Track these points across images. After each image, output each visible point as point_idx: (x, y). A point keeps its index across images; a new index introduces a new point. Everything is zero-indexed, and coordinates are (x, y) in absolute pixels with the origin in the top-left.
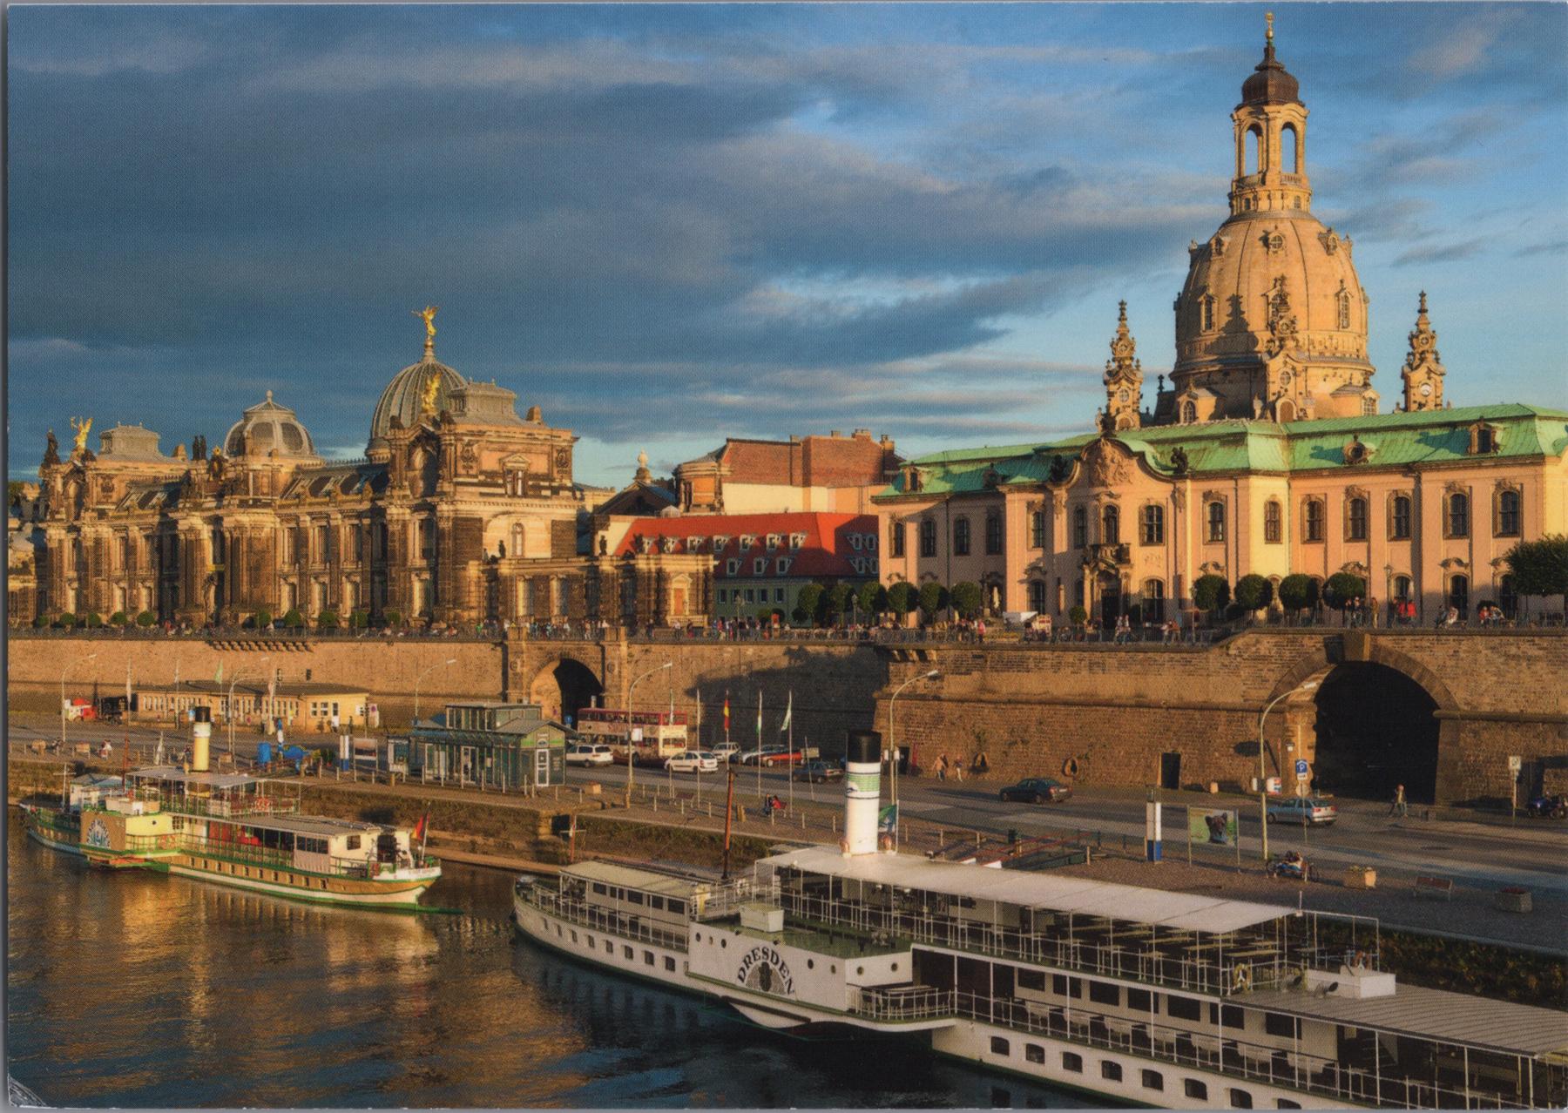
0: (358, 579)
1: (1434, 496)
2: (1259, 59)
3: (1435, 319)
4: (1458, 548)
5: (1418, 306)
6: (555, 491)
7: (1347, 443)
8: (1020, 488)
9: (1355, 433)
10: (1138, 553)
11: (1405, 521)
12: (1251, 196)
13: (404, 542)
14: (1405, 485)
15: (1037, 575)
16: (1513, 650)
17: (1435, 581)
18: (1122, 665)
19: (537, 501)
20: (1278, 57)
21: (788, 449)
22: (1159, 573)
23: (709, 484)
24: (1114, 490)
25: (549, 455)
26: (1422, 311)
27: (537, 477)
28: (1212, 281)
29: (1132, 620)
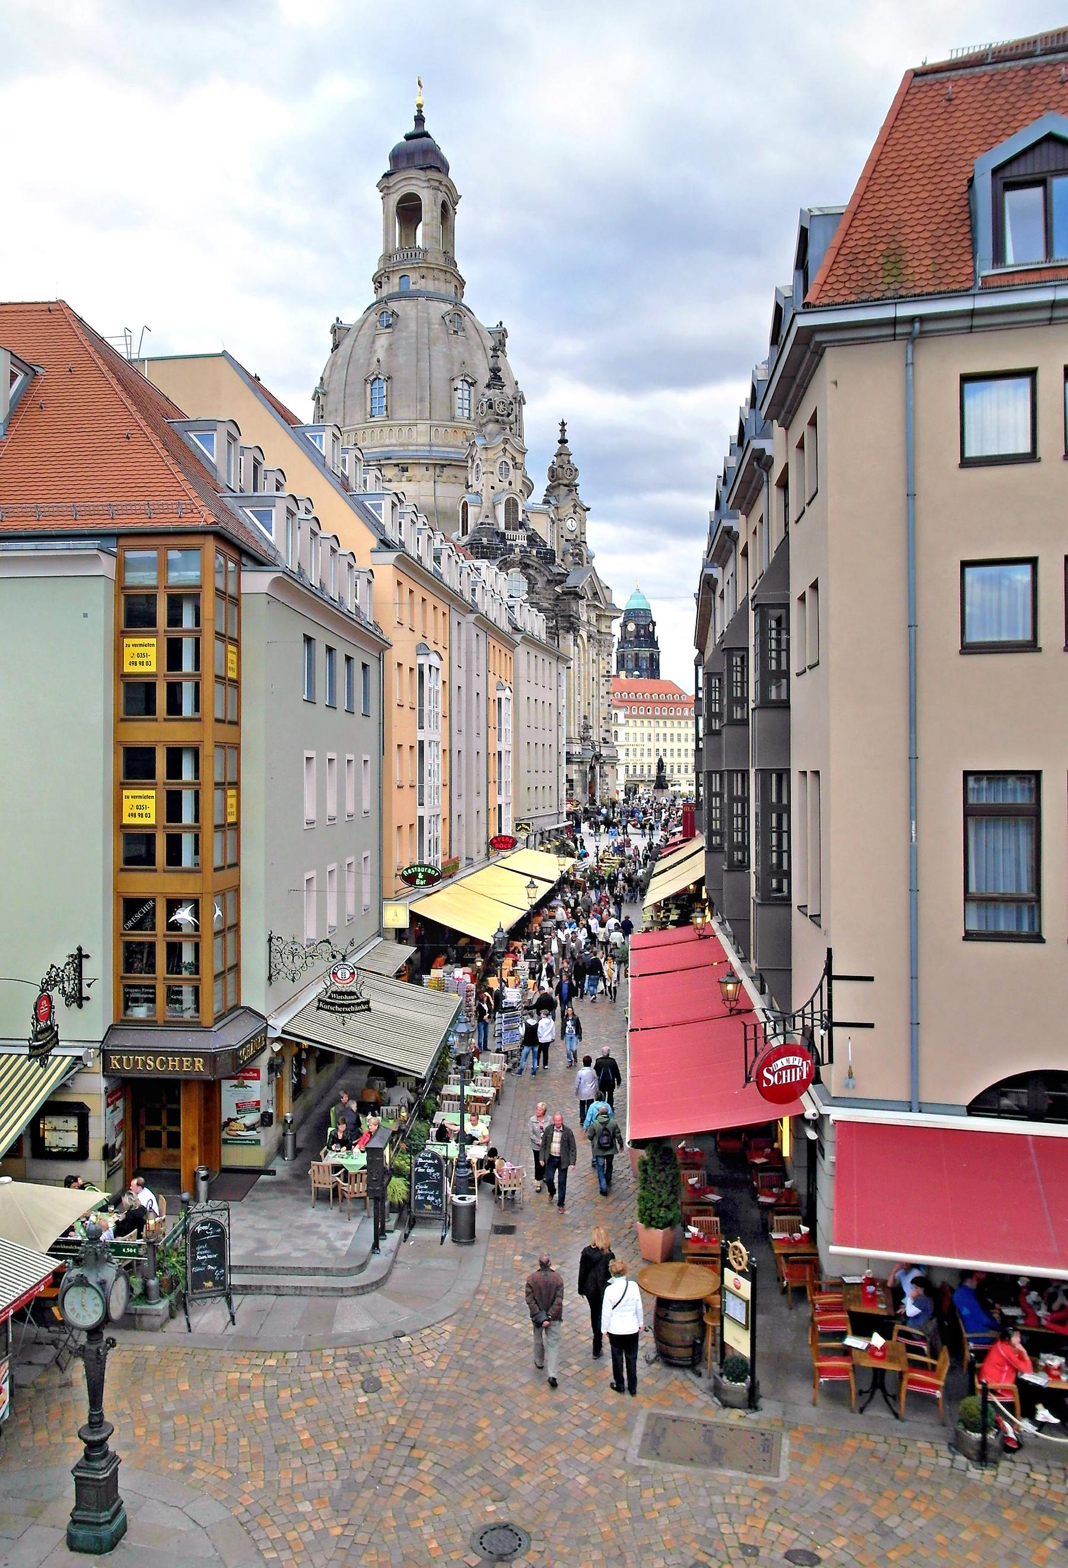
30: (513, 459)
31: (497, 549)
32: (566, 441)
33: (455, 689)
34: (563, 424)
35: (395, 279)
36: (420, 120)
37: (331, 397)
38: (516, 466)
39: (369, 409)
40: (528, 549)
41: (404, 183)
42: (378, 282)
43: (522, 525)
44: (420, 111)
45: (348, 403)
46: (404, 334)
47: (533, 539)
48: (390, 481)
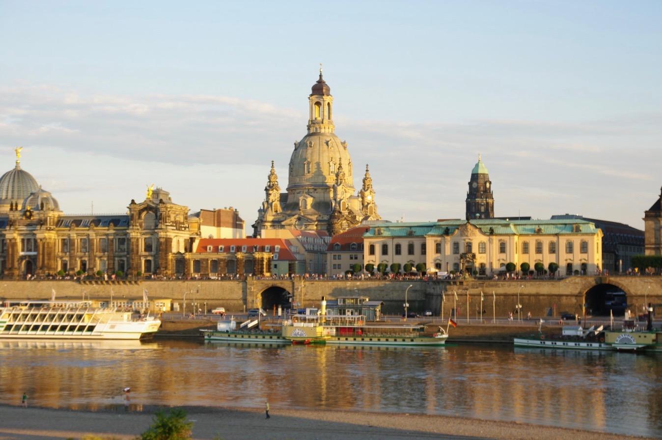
0: (106, 259)
1: (563, 242)
2: (318, 79)
3: (371, 174)
4: (570, 256)
5: (366, 169)
6: (185, 228)
7: (537, 228)
8: (433, 236)
9: (539, 225)
10: (478, 256)
11: (553, 249)
12: (318, 127)
13: (137, 246)
14: (554, 239)
15: (438, 262)
16: (646, 281)
17: (563, 264)
18: (531, 285)
19: (181, 232)
20: (324, 79)
21: (213, 213)
22: (484, 261)
23: (196, 225)
24: (471, 238)
25: (184, 215)
26: (367, 171)
27: (180, 223)
28: (309, 156)
29: (482, 274)
30: (345, 190)
36: (321, 76)
38: (346, 192)
42: (309, 128)
47: (350, 212)
48: (311, 193)
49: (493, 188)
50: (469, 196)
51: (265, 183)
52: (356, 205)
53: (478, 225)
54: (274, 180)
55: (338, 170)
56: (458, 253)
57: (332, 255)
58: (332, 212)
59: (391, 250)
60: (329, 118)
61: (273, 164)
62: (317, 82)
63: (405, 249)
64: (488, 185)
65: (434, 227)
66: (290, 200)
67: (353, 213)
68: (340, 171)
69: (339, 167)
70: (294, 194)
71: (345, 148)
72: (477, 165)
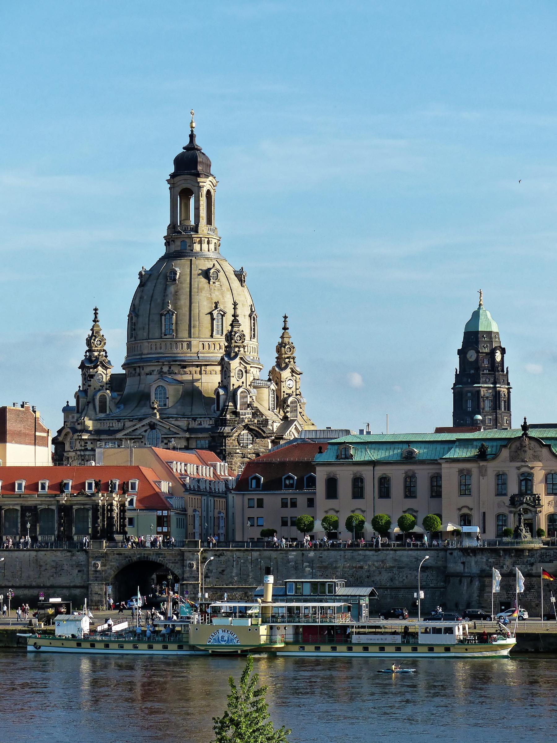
2: (186, 142)
20: (198, 142)
26: (285, 328)
31: (235, 421)
32: (288, 329)
33: (203, 518)
34: (285, 317)
35: (178, 243)
36: (192, 136)
37: (140, 319)
38: (246, 372)
39: (163, 331)
40: (253, 420)
41: (183, 181)
43: (249, 405)
44: (192, 131)
45: (151, 325)
46: (184, 285)
47: (256, 413)
49: (510, 362)
50: (459, 378)
51: (80, 354)
52: (265, 401)
53: (543, 439)
54: (99, 348)
55: (230, 328)
56: (505, 495)
57: (246, 498)
58: (218, 413)
59: (370, 488)
60: (209, 222)
61: (96, 314)
62: (184, 148)
63: (397, 488)
64: (498, 356)
65: (457, 443)
66: (130, 386)
67: (262, 415)
68: (235, 329)
69: (233, 321)
70: (139, 375)
71: (242, 281)
72: (476, 315)
